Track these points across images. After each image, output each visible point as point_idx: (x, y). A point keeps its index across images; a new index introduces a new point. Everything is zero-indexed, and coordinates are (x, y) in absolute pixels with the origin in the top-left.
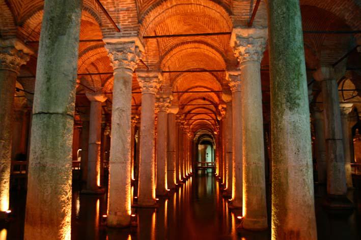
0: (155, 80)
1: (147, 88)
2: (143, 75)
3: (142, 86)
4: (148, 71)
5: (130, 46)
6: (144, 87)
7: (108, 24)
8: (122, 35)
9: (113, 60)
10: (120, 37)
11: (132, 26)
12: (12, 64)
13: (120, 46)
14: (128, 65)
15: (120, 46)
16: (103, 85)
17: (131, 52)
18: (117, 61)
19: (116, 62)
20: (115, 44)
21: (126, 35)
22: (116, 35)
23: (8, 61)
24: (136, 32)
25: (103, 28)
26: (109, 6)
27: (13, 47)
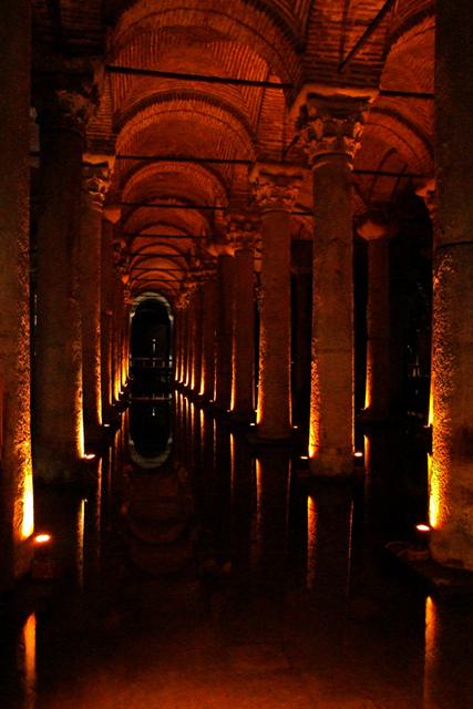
0: (298, 184)
1: (280, 200)
2: (274, 170)
3: (269, 194)
4: (284, 163)
5: (361, 108)
6: (272, 196)
7: (322, 50)
8: (346, 81)
9: (320, 134)
10: (343, 86)
11: (370, 63)
12: (82, 117)
13: (337, 106)
14: (351, 149)
15: (337, 106)
16: (122, 186)
17: (362, 123)
18: (333, 139)
19: (330, 140)
20: (327, 99)
21: (356, 83)
22: (334, 79)
23: (74, 110)
24: (375, 78)
25: (306, 59)
26: (335, 10)
27: (91, 77)
